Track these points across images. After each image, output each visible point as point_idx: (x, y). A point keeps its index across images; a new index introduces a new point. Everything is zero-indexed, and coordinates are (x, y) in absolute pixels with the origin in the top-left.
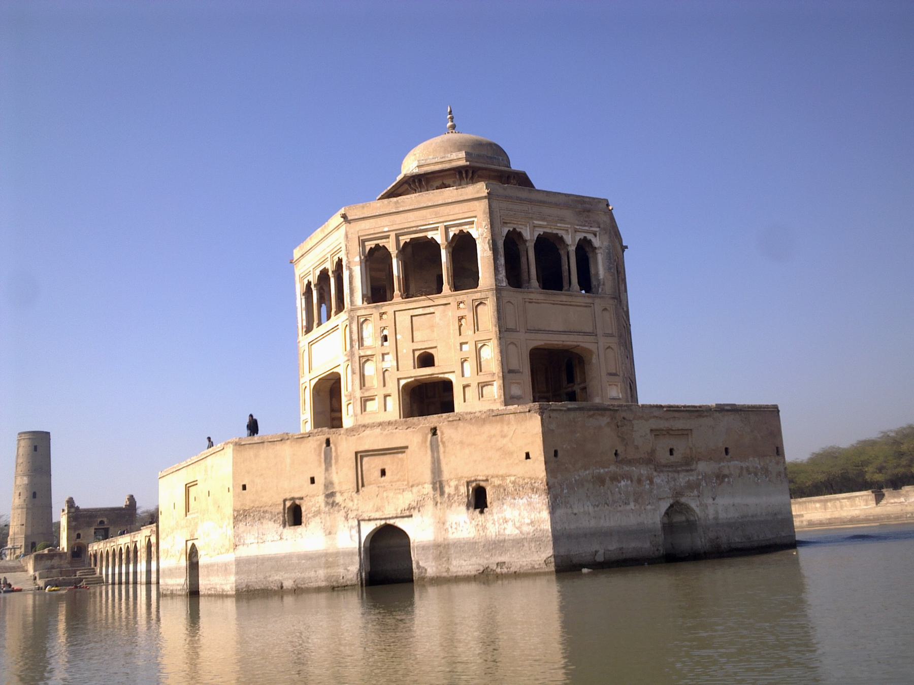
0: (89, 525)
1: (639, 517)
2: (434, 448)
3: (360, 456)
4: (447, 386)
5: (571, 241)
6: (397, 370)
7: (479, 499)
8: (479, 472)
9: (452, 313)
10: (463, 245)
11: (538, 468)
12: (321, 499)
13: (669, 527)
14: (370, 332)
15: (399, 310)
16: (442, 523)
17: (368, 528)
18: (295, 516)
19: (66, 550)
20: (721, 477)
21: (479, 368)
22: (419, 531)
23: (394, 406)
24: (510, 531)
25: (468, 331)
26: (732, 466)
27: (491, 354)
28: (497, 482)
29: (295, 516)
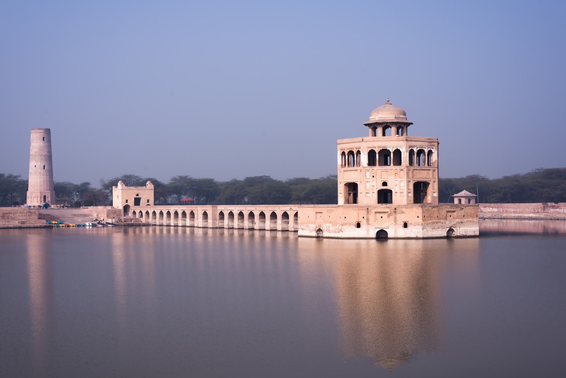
3: (376, 213)
4: (390, 191)
5: (426, 151)
7: (406, 225)
8: (406, 220)
10: (398, 153)
11: (420, 220)
12: (365, 222)
15: (377, 168)
16: (396, 231)
18: (358, 225)
20: (462, 223)
23: (375, 196)
26: (465, 220)
28: (410, 222)
29: (358, 225)
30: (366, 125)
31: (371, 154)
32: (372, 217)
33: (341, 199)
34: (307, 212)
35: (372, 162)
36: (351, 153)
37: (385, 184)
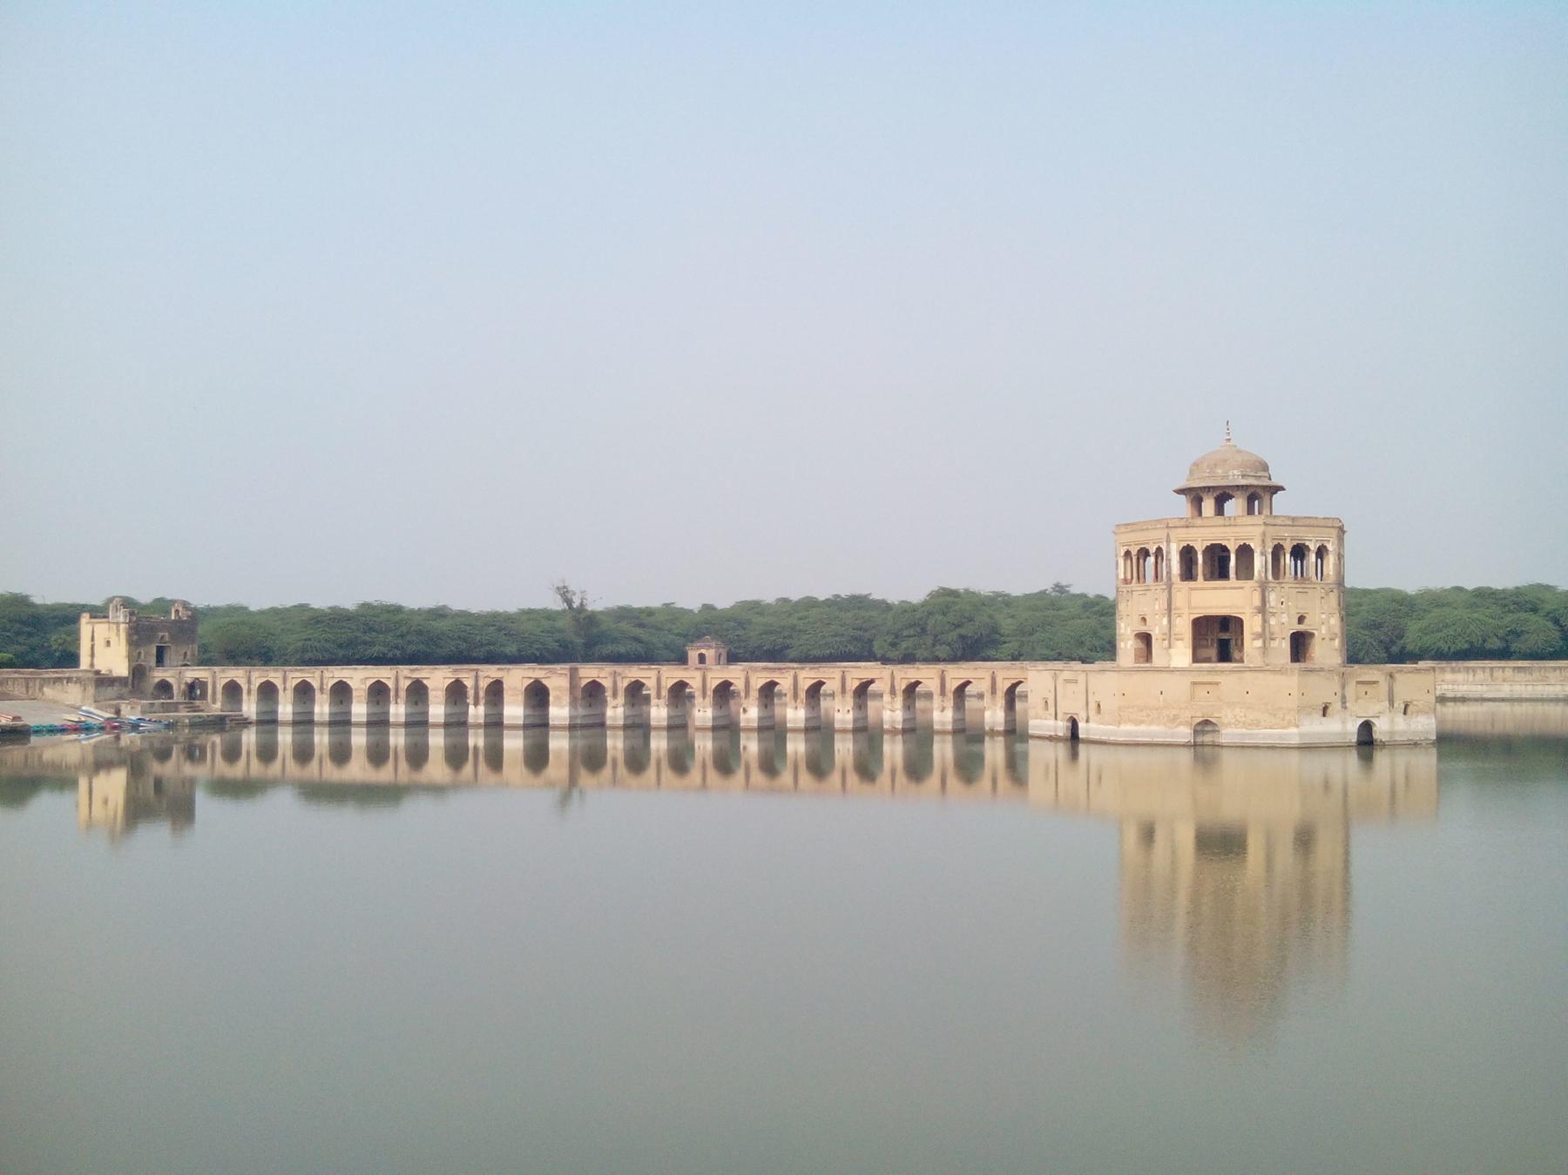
0: (150, 640)
6: (1283, 624)
12: (1338, 705)
17: (1360, 721)
19: (121, 669)
23: (1286, 645)
24: (1420, 728)
30: (1180, 491)
31: (1277, 551)
32: (1351, 691)
34: (1038, 679)
36: (1144, 553)
37: (1301, 620)
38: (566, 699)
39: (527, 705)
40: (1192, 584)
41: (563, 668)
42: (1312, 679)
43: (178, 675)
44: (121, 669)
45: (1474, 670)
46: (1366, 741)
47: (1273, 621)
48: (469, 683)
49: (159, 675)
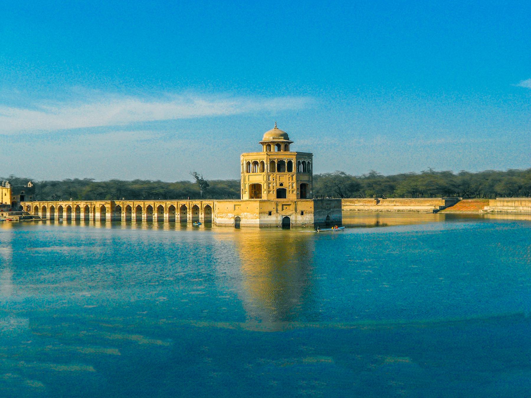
1: (322, 218)
2: (296, 205)
4: (284, 190)
5: (307, 162)
6: (275, 186)
7: (302, 214)
9: (287, 176)
10: (290, 163)
11: (313, 210)
13: (327, 219)
14: (271, 177)
16: (296, 217)
17: (284, 217)
19: (9, 203)
21: (292, 187)
22: (292, 218)
23: (275, 193)
24: (307, 219)
25: (291, 180)
27: (295, 185)
31: (272, 162)
33: (246, 196)
35: (273, 170)
37: (281, 185)
38: (110, 211)
39: (101, 213)
40: (249, 174)
41: (109, 202)
42: (264, 204)
43: (24, 204)
44: (9, 203)
45: (515, 201)
46: (286, 224)
47: (271, 185)
48: (89, 206)
49: (22, 204)
